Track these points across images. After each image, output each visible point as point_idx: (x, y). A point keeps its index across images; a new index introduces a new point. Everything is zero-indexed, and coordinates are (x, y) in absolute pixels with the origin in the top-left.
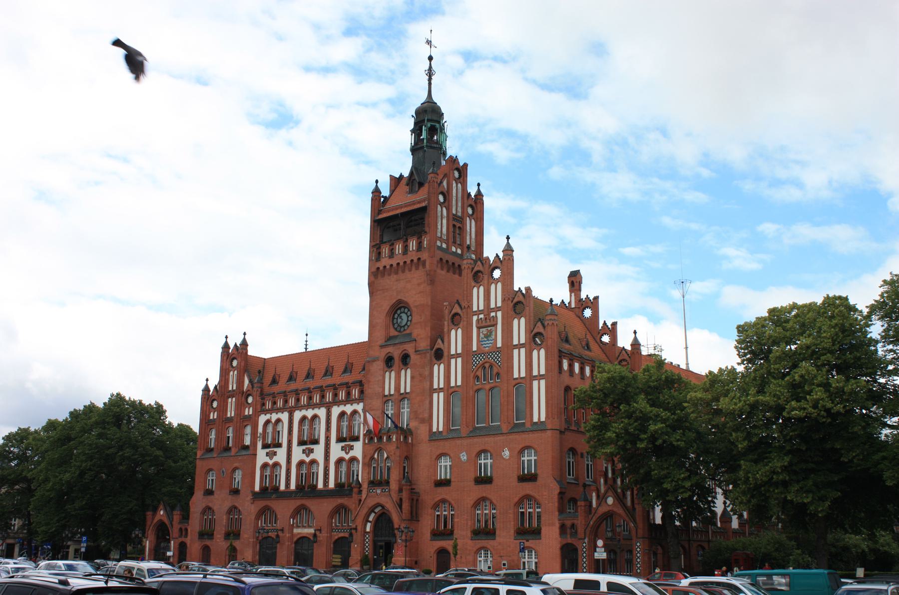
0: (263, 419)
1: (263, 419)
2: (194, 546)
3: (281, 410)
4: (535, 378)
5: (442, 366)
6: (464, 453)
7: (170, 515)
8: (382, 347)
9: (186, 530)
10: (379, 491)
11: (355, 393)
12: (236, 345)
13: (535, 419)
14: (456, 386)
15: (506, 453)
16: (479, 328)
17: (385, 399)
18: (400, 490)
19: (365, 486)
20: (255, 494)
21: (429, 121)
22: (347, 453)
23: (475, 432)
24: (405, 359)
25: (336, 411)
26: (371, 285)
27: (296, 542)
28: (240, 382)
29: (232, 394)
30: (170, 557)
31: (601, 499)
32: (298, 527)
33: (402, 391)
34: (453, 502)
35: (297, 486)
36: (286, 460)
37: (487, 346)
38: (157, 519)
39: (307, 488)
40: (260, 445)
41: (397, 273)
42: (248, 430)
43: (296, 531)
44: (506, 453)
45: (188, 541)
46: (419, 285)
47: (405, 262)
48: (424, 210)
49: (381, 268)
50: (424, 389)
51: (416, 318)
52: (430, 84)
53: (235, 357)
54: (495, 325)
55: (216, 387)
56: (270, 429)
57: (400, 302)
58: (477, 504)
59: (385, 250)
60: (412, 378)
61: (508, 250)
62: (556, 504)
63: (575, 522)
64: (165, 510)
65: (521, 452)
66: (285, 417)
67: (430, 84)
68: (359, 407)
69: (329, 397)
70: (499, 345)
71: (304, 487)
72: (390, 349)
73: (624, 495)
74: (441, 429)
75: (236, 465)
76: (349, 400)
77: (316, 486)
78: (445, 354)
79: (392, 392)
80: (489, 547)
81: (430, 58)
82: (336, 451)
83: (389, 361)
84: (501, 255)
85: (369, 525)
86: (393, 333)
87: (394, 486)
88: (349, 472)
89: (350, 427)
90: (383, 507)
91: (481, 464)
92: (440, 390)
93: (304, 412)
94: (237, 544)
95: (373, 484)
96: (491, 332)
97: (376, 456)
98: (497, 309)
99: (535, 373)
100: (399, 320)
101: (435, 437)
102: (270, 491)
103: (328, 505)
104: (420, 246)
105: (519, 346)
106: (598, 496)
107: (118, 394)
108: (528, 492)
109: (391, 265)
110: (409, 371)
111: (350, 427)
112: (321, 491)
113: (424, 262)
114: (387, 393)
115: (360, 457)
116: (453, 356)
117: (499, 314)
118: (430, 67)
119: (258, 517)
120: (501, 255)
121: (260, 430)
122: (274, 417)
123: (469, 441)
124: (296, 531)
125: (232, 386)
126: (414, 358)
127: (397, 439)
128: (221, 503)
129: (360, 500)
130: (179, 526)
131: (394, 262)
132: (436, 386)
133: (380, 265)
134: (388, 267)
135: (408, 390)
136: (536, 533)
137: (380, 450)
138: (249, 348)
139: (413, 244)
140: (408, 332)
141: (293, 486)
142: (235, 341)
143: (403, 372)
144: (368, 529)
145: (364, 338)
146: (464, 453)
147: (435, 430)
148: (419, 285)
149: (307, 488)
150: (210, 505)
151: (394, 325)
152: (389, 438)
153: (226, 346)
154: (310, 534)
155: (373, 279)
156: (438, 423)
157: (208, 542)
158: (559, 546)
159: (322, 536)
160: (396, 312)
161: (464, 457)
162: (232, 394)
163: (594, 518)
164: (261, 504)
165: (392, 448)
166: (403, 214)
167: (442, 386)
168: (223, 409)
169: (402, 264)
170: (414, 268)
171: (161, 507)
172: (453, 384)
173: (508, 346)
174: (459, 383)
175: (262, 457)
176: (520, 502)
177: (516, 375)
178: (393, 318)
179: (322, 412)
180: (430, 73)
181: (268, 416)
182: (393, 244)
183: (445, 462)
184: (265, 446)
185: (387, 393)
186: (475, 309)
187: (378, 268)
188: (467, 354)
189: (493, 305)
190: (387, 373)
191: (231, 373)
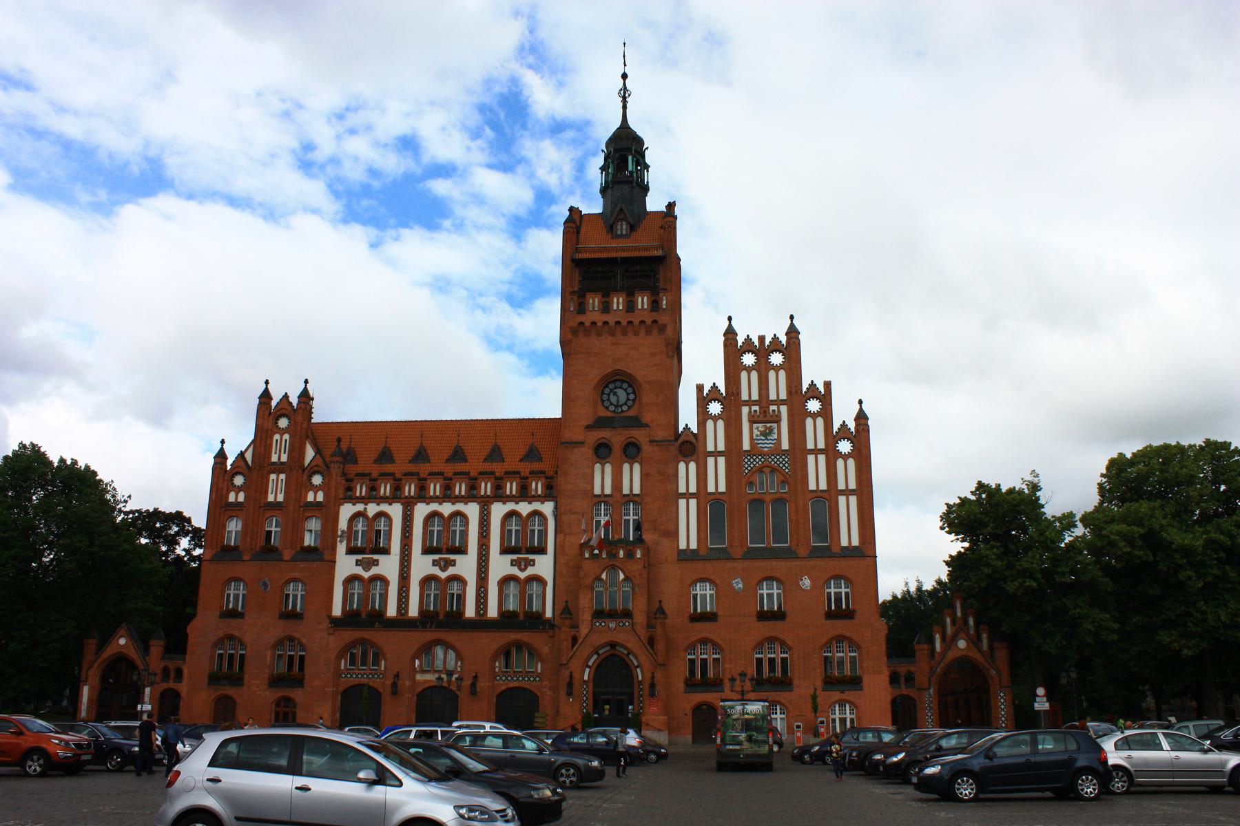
2: (197, 697)
3: (390, 500)
4: (843, 492)
5: (692, 466)
6: (739, 580)
7: (143, 643)
8: (588, 427)
9: (179, 672)
10: (612, 625)
11: (537, 487)
12: (286, 396)
13: (844, 543)
14: (717, 492)
15: (806, 583)
16: (753, 420)
17: (596, 500)
18: (650, 626)
20: (336, 622)
21: (625, 152)
22: (522, 570)
23: (752, 555)
24: (631, 451)
25: (498, 510)
26: (564, 343)
27: (421, 695)
28: (296, 452)
29: (279, 468)
30: (142, 712)
31: (949, 643)
32: (424, 672)
33: (626, 491)
34: (720, 642)
35: (421, 612)
36: (403, 574)
37: (767, 445)
38: (109, 652)
39: (443, 618)
41: (613, 334)
42: (314, 524)
43: (419, 677)
44: (806, 583)
45: (183, 688)
46: (653, 355)
47: (630, 322)
48: (660, 260)
49: (587, 324)
50: (662, 494)
51: (647, 397)
52: (625, 107)
53: (282, 416)
54: (777, 420)
55: (242, 454)
56: (360, 526)
57: (617, 372)
58: (759, 646)
59: (594, 301)
60: (644, 476)
61: (793, 332)
62: (884, 648)
63: (912, 669)
64: (130, 636)
65: (827, 583)
66: (395, 511)
67: (625, 107)
68: (547, 508)
69: (486, 488)
70: (785, 445)
71: (436, 614)
72: (605, 434)
73: (979, 639)
74: (693, 546)
75: (293, 575)
76: (524, 494)
77: (461, 613)
78: (701, 450)
79: (608, 491)
80: (782, 700)
81: (624, 76)
82: (500, 566)
83: (602, 452)
85: (587, 670)
86: (602, 412)
87: (640, 618)
88: (524, 597)
89: (523, 533)
90: (613, 645)
91: (762, 595)
92: (687, 496)
93: (434, 507)
94: (297, 694)
95: (599, 614)
96: (771, 430)
97: (604, 576)
98: (779, 402)
99: (841, 486)
100: (613, 399)
101: (687, 556)
102: (364, 618)
103: (492, 641)
104: (655, 305)
105: (816, 452)
106: (943, 638)
107: (33, 445)
108: (841, 632)
109: (606, 323)
110: (637, 467)
112: (470, 620)
113: (662, 329)
114: (597, 491)
115: (548, 575)
116: (711, 454)
117: (784, 409)
118: (625, 88)
119: (341, 655)
120: (783, 339)
121: (343, 524)
122: (372, 509)
123: (746, 564)
124: (419, 677)
125: (279, 455)
126: (647, 448)
127: (643, 555)
128: (259, 634)
129: (575, 640)
130: (162, 665)
131: (611, 319)
132: (682, 489)
133: (587, 319)
134: (600, 324)
135: (637, 490)
136: (854, 682)
137: (613, 568)
138: (314, 404)
139: (642, 301)
140: (631, 413)
141: (413, 611)
142: (286, 387)
143: (626, 467)
144: (586, 678)
145: (556, 413)
146: (739, 580)
147: (683, 546)
148: (653, 355)
149: (443, 618)
150: (236, 633)
151: (603, 401)
152: (630, 555)
153: (266, 396)
155: (570, 336)
156: (688, 535)
157: (230, 691)
158: (890, 698)
159: (483, 684)
160: (607, 386)
161: (738, 585)
162: (279, 468)
163: (942, 665)
164: (350, 635)
165: (635, 568)
166: (625, 260)
167: (693, 489)
168: (256, 486)
169: (624, 323)
170: (643, 332)
171: (123, 632)
172: (711, 489)
173: (799, 451)
174: (722, 488)
175: (346, 565)
176: (827, 646)
177: (812, 486)
178: (603, 393)
179: (472, 510)
180: (624, 95)
181: (360, 507)
182: (633, 295)
183: (704, 592)
184: (351, 551)
185: (597, 491)
186: (745, 397)
187: (582, 324)
188: (733, 451)
189: (773, 396)
190: (598, 466)
191: (277, 437)
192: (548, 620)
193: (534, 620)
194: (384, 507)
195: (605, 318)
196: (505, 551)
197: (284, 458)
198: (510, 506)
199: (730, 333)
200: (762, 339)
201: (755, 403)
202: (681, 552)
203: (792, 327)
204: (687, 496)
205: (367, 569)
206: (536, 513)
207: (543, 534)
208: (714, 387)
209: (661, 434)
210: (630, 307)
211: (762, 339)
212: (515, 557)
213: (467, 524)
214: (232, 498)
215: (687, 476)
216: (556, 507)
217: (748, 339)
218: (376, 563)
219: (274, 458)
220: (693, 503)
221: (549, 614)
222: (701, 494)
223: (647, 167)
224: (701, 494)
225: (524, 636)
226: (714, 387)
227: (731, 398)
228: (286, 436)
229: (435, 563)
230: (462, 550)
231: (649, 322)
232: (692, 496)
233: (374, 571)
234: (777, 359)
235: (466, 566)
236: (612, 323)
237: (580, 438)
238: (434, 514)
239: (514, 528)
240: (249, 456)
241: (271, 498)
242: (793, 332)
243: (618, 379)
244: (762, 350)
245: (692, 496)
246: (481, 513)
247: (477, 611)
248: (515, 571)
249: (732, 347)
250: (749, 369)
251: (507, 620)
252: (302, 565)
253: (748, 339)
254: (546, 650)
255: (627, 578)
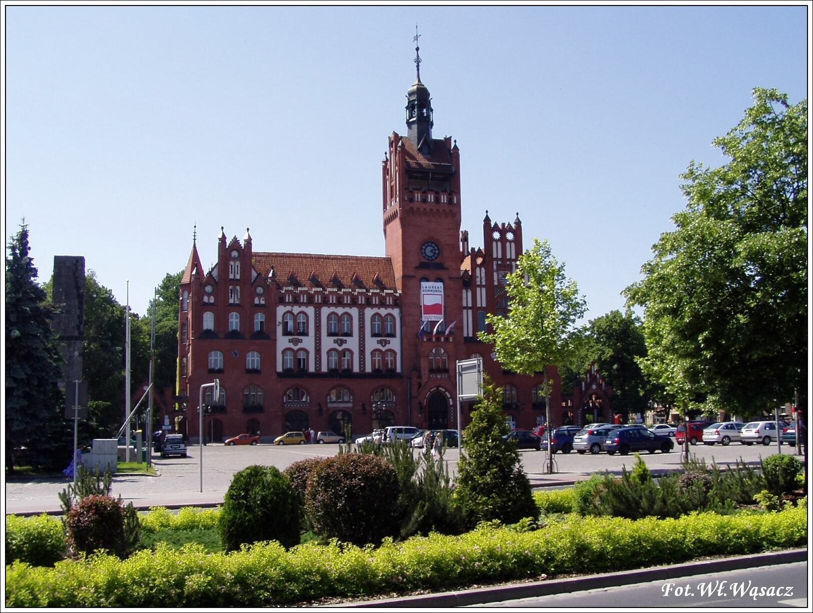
0: (281, 310)
1: (281, 310)
3: (307, 304)
8: (417, 268)
19: (425, 372)
20: (279, 374)
21: (420, 102)
36: (318, 348)
40: (279, 329)
43: (329, 405)
46: (449, 229)
47: (438, 210)
52: (418, 70)
59: (418, 196)
67: (418, 70)
68: (396, 312)
81: (417, 49)
82: (372, 344)
84: (513, 226)
92: (467, 308)
95: (431, 371)
111: (383, 327)
120: (513, 226)
121: (279, 319)
125: (235, 274)
129: (420, 385)
133: (415, 206)
139: (444, 199)
140: (436, 261)
142: (237, 233)
148: (449, 229)
154: (348, 408)
164: (290, 382)
167: (470, 305)
172: (479, 305)
175: (283, 342)
181: (288, 308)
184: (286, 333)
186: (495, 256)
187: (412, 208)
189: (508, 257)
192: (398, 374)
193: (391, 373)
194: (303, 308)
195: (424, 206)
196: (374, 335)
197: (238, 277)
198: (376, 310)
199: (487, 220)
200: (503, 224)
201: (500, 259)
202: (465, 338)
203: (518, 218)
204: (467, 308)
205: (296, 345)
206: (389, 314)
207: (394, 326)
208: (479, 249)
209: (454, 275)
210: (437, 200)
211: (503, 224)
212: (379, 339)
213: (352, 320)
214: (206, 299)
215: (467, 297)
216: (401, 312)
217: (496, 224)
218: (301, 341)
219: (231, 276)
220: (470, 312)
221: (399, 370)
222: (474, 308)
223: (432, 110)
224: (474, 308)
225: (387, 382)
226: (479, 249)
227: (487, 254)
228: (238, 263)
229: (335, 342)
230: (350, 335)
231: (447, 210)
232: (470, 308)
233: (300, 346)
234: (510, 236)
235: (352, 343)
236: (428, 209)
237: (412, 274)
238: (333, 313)
239: (377, 323)
240: (215, 274)
241: (231, 301)
242: (518, 223)
243: (430, 241)
244: (503, 231)
245: (470, 308)
246: (360, 315)
247: (360, 368)
248: (379, 347)
249: (488, 228)
250: (497, 241)
251: (377, 373)
252: (258, 342)
253: (496, 224)
254: (399, 389)
255: (445, 352)
